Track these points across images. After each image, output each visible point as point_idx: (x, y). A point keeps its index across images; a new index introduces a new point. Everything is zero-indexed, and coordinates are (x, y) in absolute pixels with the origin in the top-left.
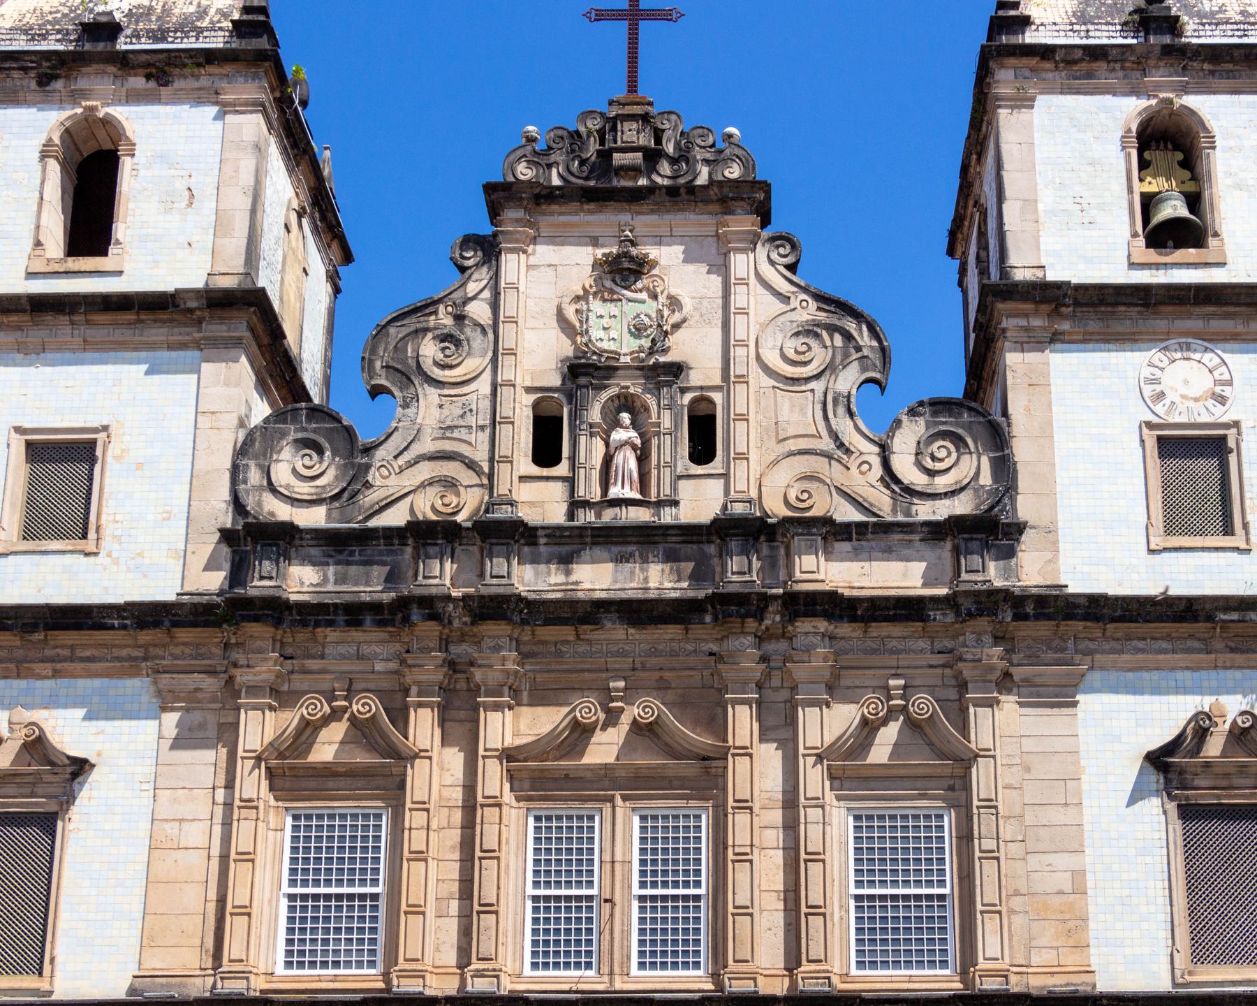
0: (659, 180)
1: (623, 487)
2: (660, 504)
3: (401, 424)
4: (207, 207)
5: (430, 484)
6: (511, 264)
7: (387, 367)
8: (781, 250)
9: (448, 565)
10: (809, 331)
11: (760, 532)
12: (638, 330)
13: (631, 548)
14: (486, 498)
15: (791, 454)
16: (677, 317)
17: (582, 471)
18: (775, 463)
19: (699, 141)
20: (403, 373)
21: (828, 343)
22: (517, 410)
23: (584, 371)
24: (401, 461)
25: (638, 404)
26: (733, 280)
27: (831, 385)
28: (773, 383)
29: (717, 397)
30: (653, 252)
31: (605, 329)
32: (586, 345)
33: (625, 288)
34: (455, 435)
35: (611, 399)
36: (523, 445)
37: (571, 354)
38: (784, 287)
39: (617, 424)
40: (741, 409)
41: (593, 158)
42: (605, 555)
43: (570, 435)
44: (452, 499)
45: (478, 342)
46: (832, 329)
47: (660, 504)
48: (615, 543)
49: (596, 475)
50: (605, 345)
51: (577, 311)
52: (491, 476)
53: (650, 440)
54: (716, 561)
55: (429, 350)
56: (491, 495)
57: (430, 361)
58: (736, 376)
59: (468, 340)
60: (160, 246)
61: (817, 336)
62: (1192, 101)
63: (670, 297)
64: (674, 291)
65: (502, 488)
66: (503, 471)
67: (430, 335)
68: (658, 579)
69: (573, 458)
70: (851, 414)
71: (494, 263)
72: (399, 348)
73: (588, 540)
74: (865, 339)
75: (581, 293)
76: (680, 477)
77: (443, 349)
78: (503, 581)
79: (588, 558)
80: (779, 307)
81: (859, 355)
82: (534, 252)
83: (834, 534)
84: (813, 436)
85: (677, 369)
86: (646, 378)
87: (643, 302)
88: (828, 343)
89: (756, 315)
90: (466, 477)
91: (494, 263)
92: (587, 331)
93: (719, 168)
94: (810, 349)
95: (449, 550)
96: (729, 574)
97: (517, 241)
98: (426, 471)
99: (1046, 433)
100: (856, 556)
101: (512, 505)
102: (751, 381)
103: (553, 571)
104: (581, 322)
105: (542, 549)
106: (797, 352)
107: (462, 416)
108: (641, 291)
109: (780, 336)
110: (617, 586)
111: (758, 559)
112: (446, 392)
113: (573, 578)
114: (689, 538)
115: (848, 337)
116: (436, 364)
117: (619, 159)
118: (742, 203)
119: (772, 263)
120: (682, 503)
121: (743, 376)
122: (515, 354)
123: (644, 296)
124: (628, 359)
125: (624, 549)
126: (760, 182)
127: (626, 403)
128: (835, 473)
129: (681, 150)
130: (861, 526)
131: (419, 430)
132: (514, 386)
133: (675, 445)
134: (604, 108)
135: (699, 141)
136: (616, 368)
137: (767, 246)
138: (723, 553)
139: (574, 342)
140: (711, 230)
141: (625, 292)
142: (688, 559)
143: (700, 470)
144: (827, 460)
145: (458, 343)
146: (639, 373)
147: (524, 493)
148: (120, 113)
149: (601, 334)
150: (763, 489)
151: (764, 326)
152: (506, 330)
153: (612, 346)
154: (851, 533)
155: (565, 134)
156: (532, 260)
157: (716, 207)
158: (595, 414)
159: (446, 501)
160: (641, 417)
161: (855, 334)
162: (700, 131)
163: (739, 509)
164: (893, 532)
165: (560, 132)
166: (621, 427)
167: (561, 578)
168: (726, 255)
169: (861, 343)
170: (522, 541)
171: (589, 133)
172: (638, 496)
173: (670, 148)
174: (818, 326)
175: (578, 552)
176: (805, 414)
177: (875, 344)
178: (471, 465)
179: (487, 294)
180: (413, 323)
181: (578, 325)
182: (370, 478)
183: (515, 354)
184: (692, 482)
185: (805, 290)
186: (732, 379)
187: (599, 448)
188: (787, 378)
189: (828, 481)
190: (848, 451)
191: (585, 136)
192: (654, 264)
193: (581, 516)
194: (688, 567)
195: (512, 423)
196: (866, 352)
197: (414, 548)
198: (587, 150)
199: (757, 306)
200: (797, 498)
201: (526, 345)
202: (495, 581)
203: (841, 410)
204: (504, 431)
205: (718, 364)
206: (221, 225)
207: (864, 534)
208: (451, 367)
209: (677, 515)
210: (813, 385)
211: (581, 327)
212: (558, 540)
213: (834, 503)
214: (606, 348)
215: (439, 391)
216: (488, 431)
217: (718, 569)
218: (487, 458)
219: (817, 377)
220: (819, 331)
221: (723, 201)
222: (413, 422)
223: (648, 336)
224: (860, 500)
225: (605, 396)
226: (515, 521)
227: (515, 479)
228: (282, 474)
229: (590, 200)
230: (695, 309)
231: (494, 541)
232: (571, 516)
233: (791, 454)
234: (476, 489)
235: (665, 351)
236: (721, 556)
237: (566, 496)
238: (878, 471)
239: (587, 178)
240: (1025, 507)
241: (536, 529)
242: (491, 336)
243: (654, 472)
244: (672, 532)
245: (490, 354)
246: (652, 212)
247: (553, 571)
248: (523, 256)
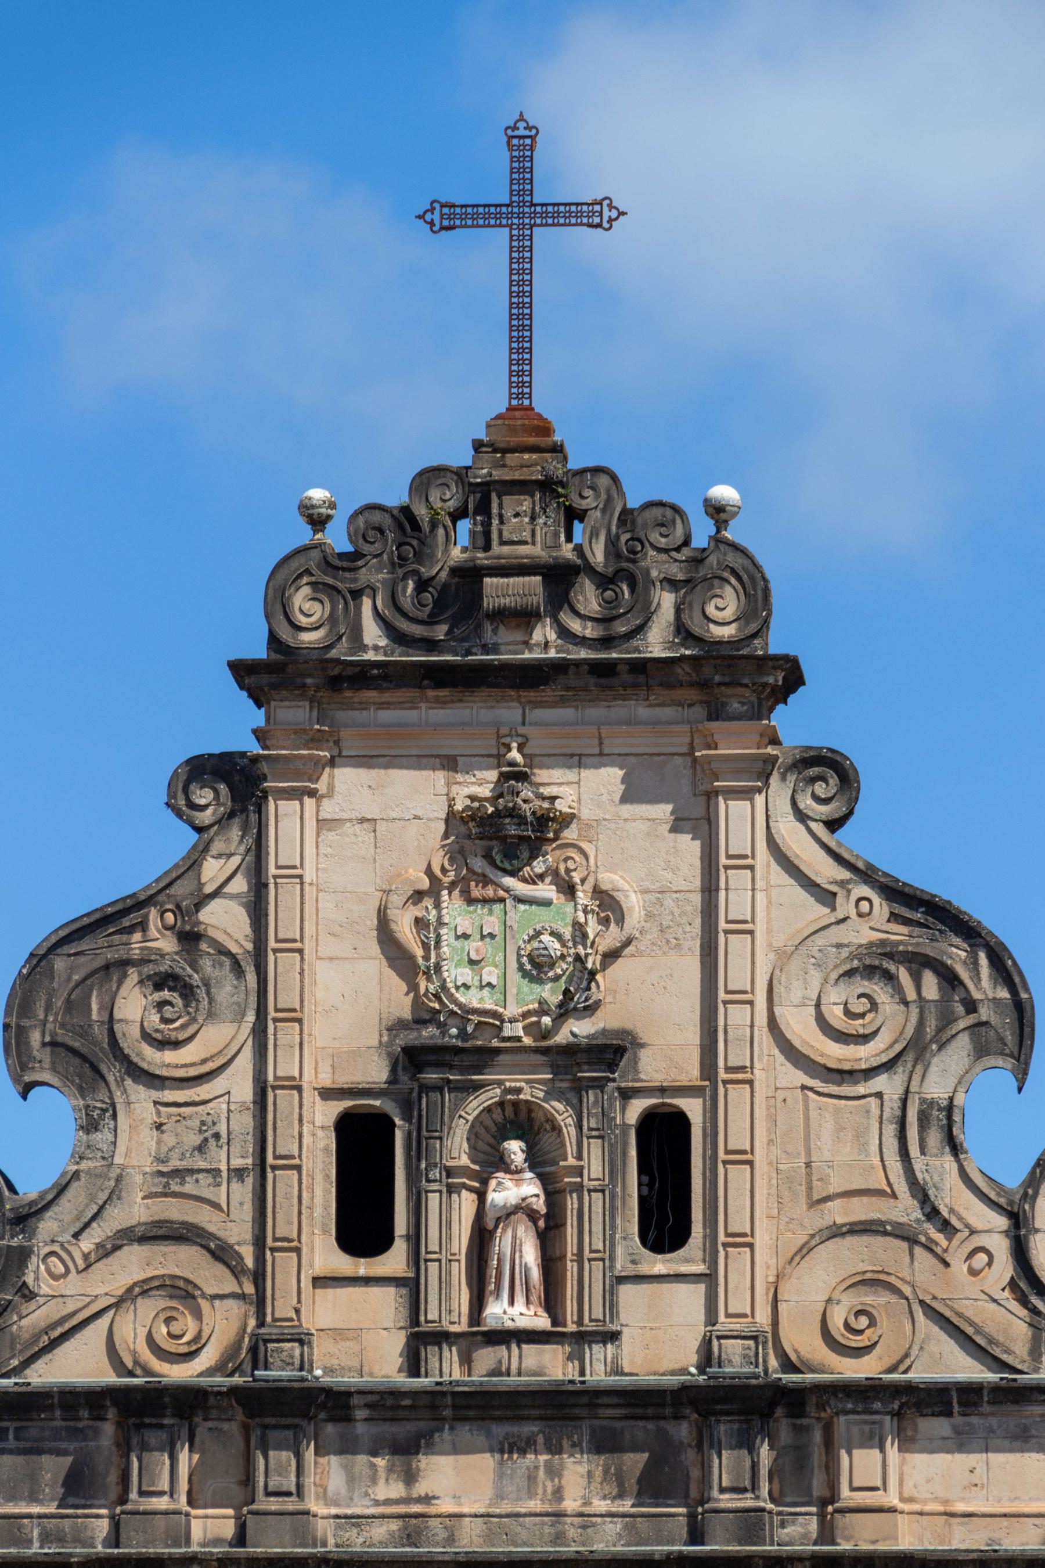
0: (575, 626)
1: (512, 1302)
2: (582, 1339)
3: (84, 1165)
5: (144, 1293)
6: (287, 822)
7: (54, 1044)
8: (820, 788)
9: (184, 1457)
10: (873, 965)
11: (773, 1404)
12: (537, 967)
13: (529, 1428)
14: (252, 1323)
15: (836, 1232)
16: (612, 937)
17: (433, 1267)
18: (804, 1251)
19: (655, 537)
20: (84, 1058)
21: (911, 995)
22: (306, 1141)
23: (435, 1054)
24: (87, 1244)
25: (539, 1116)
26: (723, 860)
27: (913, 1088)
28: (801, 1078)
29: (693, 1108)
30: (566, 788)
31: (472, 962)
32: (437, 996)
33: (512, 874)
34: (188, 1188)
35: (488, 1110)
36: (318, 1212)
37: (407, 1014)
38: (825, 871)
39: (500, 1163)
40: (738, 1140)
41: (444, 575)
42: (481, 1440)
43: (409, 1189)
44: (188, 1325)
45: (227, 991)
46: (918, 962)
47: (582, 1339)
48: (500, 1419)
49: (459, 1272)
50: (473, 999)
51: (417, 921)
52: (259, 1276)
53: (561, 1192)
54: (690, 1456)
55: (133, 1006)
56: (261, 1324)
57: (135, 1032)
58: (728, 1069)
59: (207, 985)
61: (890, 977)
63: (598, 892)
64: (608, 879)
65: (281, 1307)
66: (283, 1269)
67: (133, 976)
69: (415, 1239)
70: (955, 1148)
71: (253, 818)
72: (76, 1006)
73: (447, 1413)
74: (984, 986)
75: (425, 884)
76: (621, 1280)
77: (161, 1005)
78: (290, 1504)
79: (448, 1446)
80: (820, 912)
81: (971, 1020)
82: (330, 793)
83: (918, 1405)
84: (879, 1193)
85: (612, 1052)
86: (556, 1069)
87: (547, 903)
88: (911, 995)
89: (769, 931)
90: (212, 1278)
91: (253, 818)
92: (438, 968)
93: (696, 597)
94: (874, 1006)
95: (185, 1432)
96: (715, 1493)
97: (297, 776)
98: (134, 1265)
100: (960, 1443)
101: (301, 1342)
102: (759, 1075)
103: (382, 1474)
104: (426, 946)
105: (360, 1428)
106: (848, 1013)
107: (201, 1148)
108: (541, 877)
109: (815, 978)
110: (506, 1507)
111: (772, 1447)
112: (169, 1096)
113: (421, 1488)
114: (639, 1411)
115: (950, 979)
116: (146, 1036)
117: (498, 591)
118: (740, 690)
119: (801, 817)
120: (625, 1337)
121: (742, 1069)
122: (300, 1021)
123: (547, 890)
124: (518, 1030)
125: (514, 1429)
126: (775, 658)
127: (519, 1120)
128: (920, 1272)
129: (618, 556)
130: (969, 1395)
131: (119, 1179)
132: (299, 1089)
133: (611, 1213)
134: (463, 457)
135: (655, 537)
136: (497, 1051)
137: (792, 778)
138: (705, 1443)
139: (413, 987)
140: (680, 743)
141: (509, 881)
142: (635, 1448)
143: (660, 1264)
144: (905, 1245)
145: (187, 992)
146: (540, 1059)
147: (325, 1311)
149: (465, 975)
150: (782, 1307)
151: (783, 957)
152: (282, 967)
153: (487, 1001)
154: (950, 1404)
155: (387, 521)
156: (329, 809)
157: (692, 694)
158: (457, 1149)
159: (176, 1328)
160: (547, 1140)
161: (964, 975)
162: (657, 512)
163: (734, 1349)
164: (1030, 1402)
165: (376, 517)
166: (508, 1171)
167: (396, 1490)
168: (711, 795)
169: (976, 995)
170: (322, 1415)
171: (434, 524)
172: (542, 1322)
173: (598, 555)
174: (890, 956)
175: (431, 1434)
176: (864, 1147)
177: (1004, 994)
178: (221, 1253)
179: (240, 885)
180: (102, 948)
181: (419, 952)
182: (29, 1279)
183: (300, 1021)
184: (645, 1288)
185: (866, 874)
186: (722, 1075)
187: (467, 1203)
188: (830, 1070)
189: (907, 1290)
190: (946, 1227)
191: (426, 527)
192: (566, 820)
193: (434, 1363)
194: (635, 1461)
195: (298, 1168)
196: (985, 1013)
197: (119, 1425)
198: (432, 556)
199: (770, 909)
200: (847, 1325)
201: (320, 994)
202: (274, 1504)
203: (935, 1137)
204: (282, 1185)
205: (692, 1036)
207: (976, 1405)
208: (176, 1044)
209: (616, 1358)
210: (880, 1083)
211: (427, 958)
212: (390, 1414)
213: (920, 1336)
214: (475, 1004)
215: (155, 1095)
216: (249, 1181)
217: (695, 1473)
218: (249, 1236)
219: (888, 1066)
220: (892, 967)
221: (704, 685)
222: (108, 1160)
223: (557, 978)
224: (970, 1331)
225: (475, 1106)
226: (309, 1389)
227: (306, 1283)
229: (439, 685)
230: (649, 916)
231: (272, 1421)
232: (413, 1364)
233: (836, 1232)
234: (231, 1303)
235: (591, 1009)
236: (699, 1446)
237: (403, 1320)
238: (1004, 1268)
239: (431, 621)
241: (348, 1394)
242: (251, 978)
243: (571, 1268)
244: (605, 1400)
245: (251, 1017)
246: (562, 702)
247: (382, 1474)
248: (309, 803)
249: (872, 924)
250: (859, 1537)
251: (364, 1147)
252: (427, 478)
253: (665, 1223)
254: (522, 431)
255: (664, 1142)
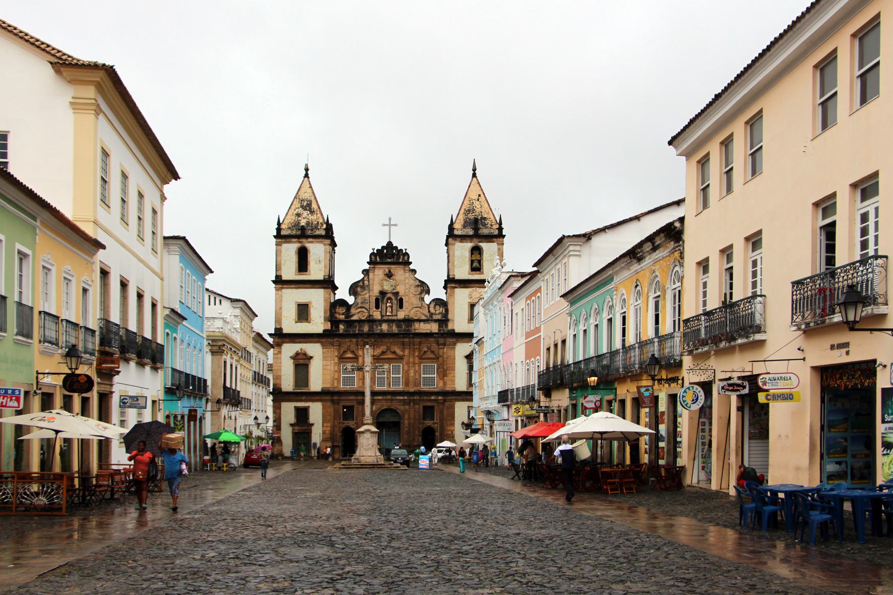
4: (323, 263)
6: (371, 275)
10: (418, 286)
23: (383, 293)
60: (316, 272)
62: (481, 244)
68: (395, 329)
98: (359, 310)
99: (454, 303)
127: (389, 298)
148: (308, 245)
206: (325, 267)
228: (337, 310)
240: (450, 317)
249: (418, 283)
250: (417, 331)
251: (377, 300)
252: (383, 247)
253: (401, 307)
254: (390, 243)
255: (401, 300)
